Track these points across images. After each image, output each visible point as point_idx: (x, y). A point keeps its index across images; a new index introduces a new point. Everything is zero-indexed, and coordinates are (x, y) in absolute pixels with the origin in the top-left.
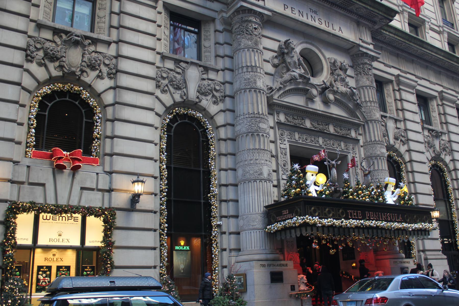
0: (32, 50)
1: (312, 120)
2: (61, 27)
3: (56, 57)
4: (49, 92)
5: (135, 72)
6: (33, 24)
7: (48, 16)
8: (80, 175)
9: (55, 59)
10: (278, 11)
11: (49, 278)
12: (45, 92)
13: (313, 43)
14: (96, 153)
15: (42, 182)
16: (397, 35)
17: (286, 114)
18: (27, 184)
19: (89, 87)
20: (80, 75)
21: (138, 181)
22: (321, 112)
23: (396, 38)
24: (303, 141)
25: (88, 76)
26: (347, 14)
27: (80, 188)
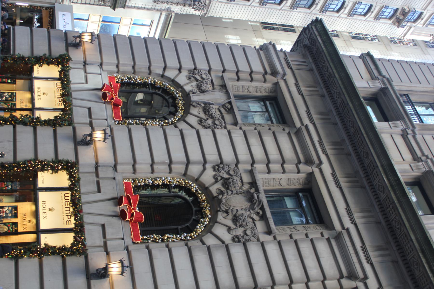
0: (225, 168)
2: (259, 185)
3: (228, 186)
4: (193, 190)
5: (253, 261)
6: (249, 168)
7: (267, 185)
8: (117, 222)
9: (227, 186)
11: (4, 216)
12: (191, 186)
14: (146, 239)
15: (102, 189)
18: (97, 179)
19: (214, 221)
20: (222, 210)
21: (123, 266)
25: (224, 218)
27: (103, 223)
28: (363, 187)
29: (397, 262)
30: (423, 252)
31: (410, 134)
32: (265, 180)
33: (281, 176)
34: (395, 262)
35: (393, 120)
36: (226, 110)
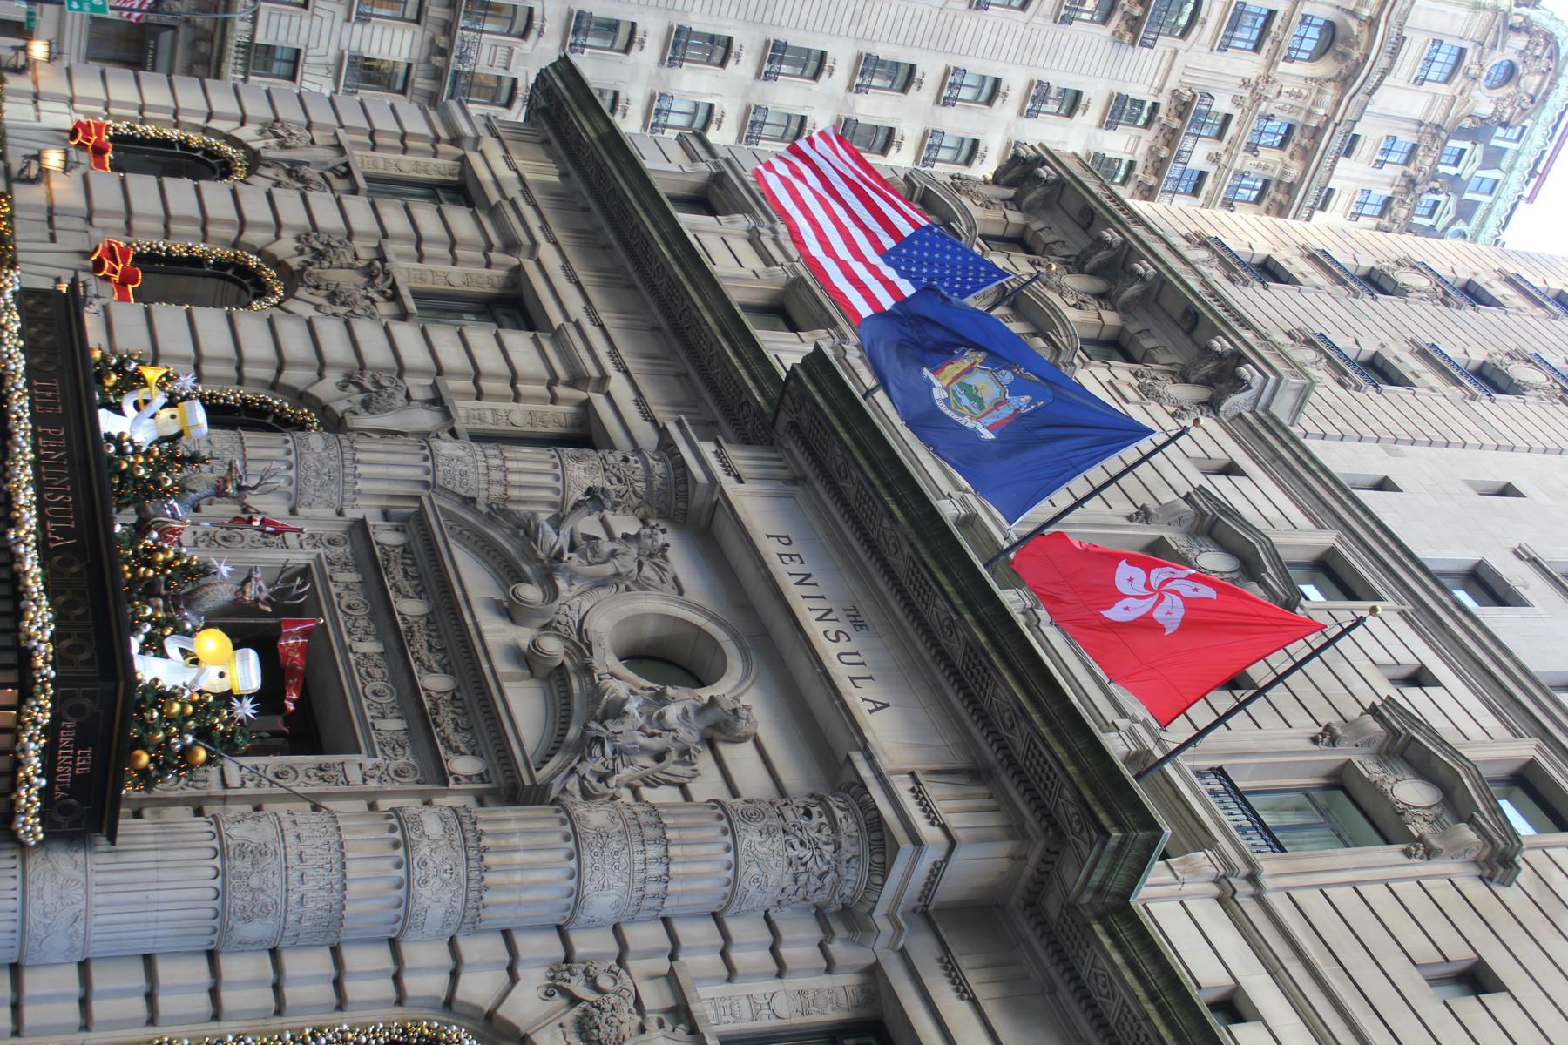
1: (430, 619)
10: (739, 511)
13: (752, 653)
16: (1161, 1009)
17: (406, 549)
22: (468, 620)
23: (1147, 1018)
24: (338, 595)
26: (969, 722)
28: (631, 286)
29: (687, 375)
30: (726, 335)
31: (765, 234)
32: (412, 273)
33: (449, 268)
34: (682, 376)
35: (726, 213)
36: (337, 176)
